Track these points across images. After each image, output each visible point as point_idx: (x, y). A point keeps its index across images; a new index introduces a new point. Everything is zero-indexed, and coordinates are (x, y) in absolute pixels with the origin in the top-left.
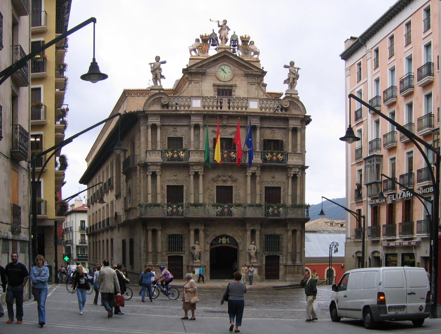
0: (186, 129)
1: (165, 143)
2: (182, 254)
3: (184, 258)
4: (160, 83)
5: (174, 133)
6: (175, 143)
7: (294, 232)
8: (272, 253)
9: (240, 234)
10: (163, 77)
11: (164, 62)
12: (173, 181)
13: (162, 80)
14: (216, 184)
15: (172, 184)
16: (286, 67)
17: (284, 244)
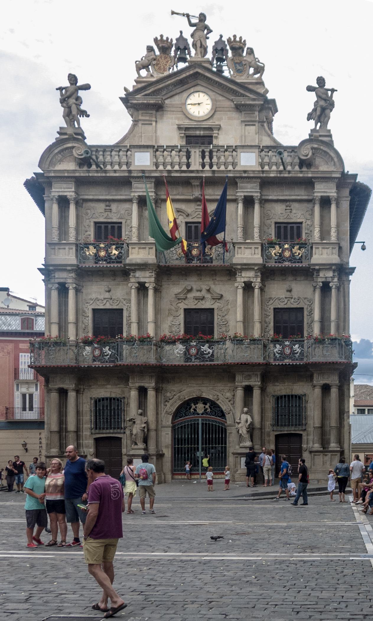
0: (127, 206)
1: (88, 233)
2: (121, 433)
3: (124, 442)
4: (79, 124)
5: (105, 214)
6: (109, 232)
7: (326, 389)
8: (286, 430)
9: (229, 395)
10: (84, 113)
11: (87, 87)
12: (105, 301)
13: (83, 120)
14: (183, 306)
15: (101, 307)
16: (310, 89)
17: (310, 413)
